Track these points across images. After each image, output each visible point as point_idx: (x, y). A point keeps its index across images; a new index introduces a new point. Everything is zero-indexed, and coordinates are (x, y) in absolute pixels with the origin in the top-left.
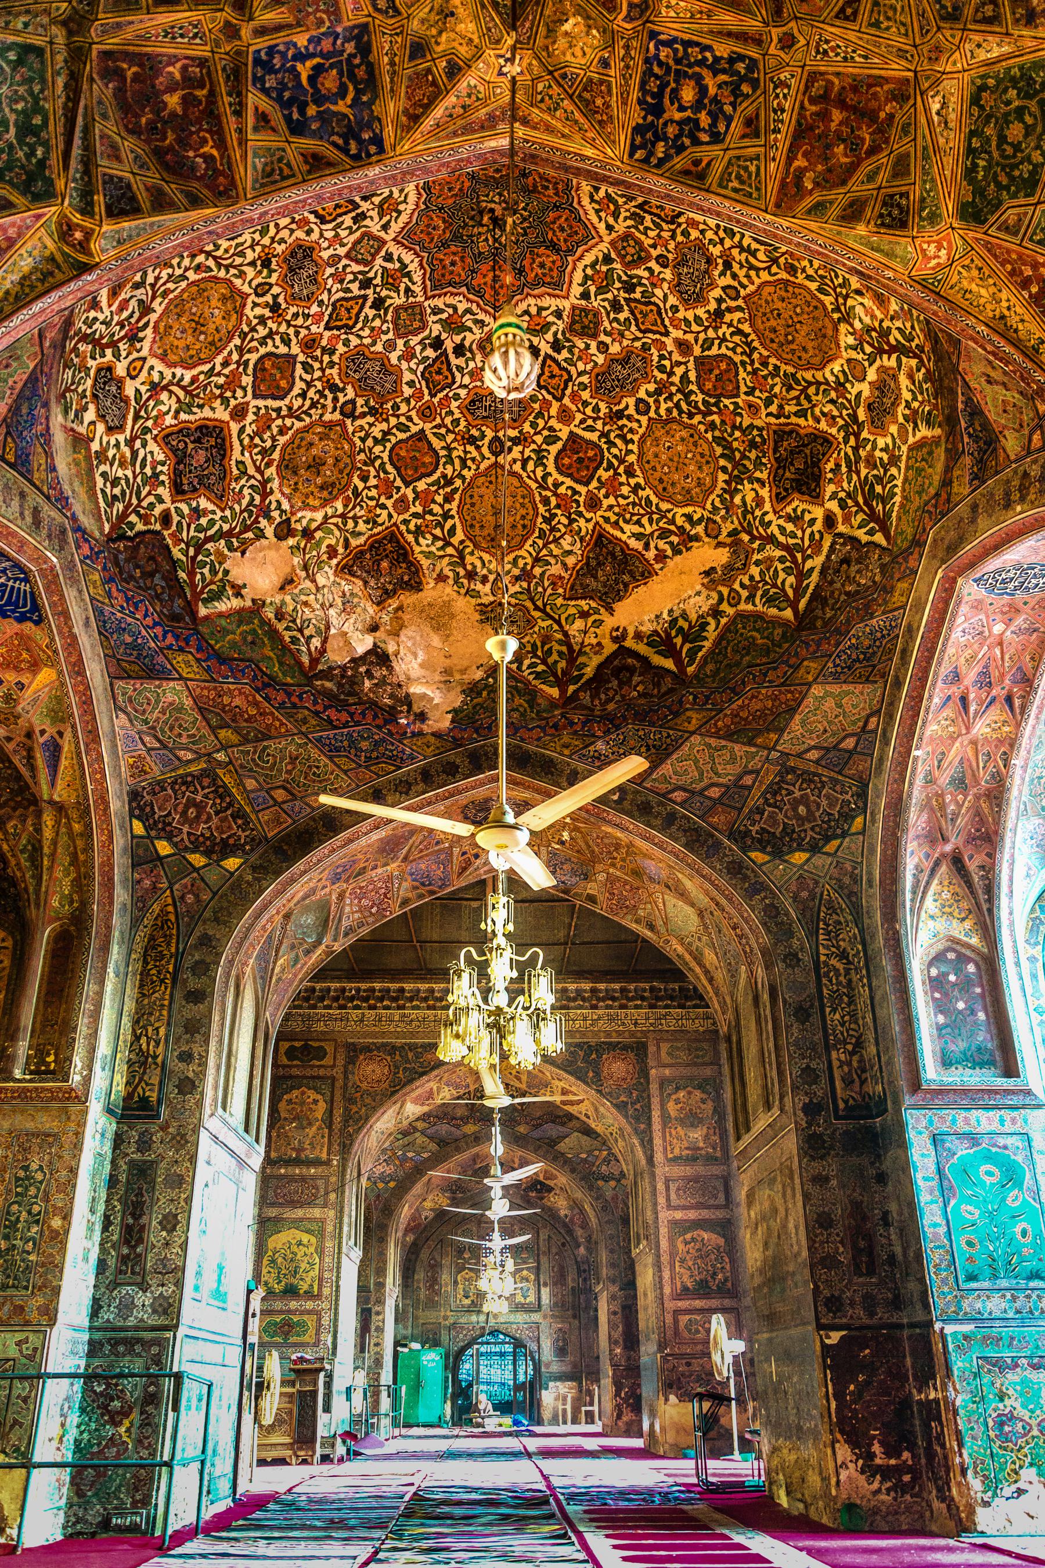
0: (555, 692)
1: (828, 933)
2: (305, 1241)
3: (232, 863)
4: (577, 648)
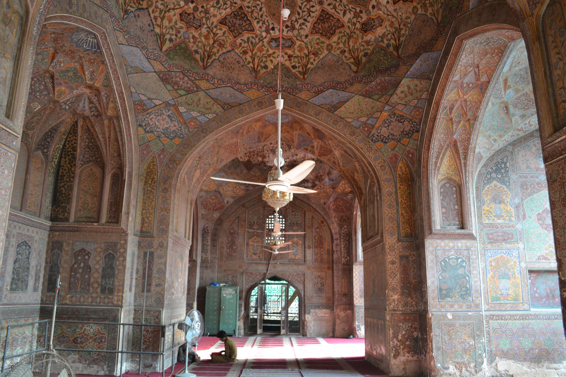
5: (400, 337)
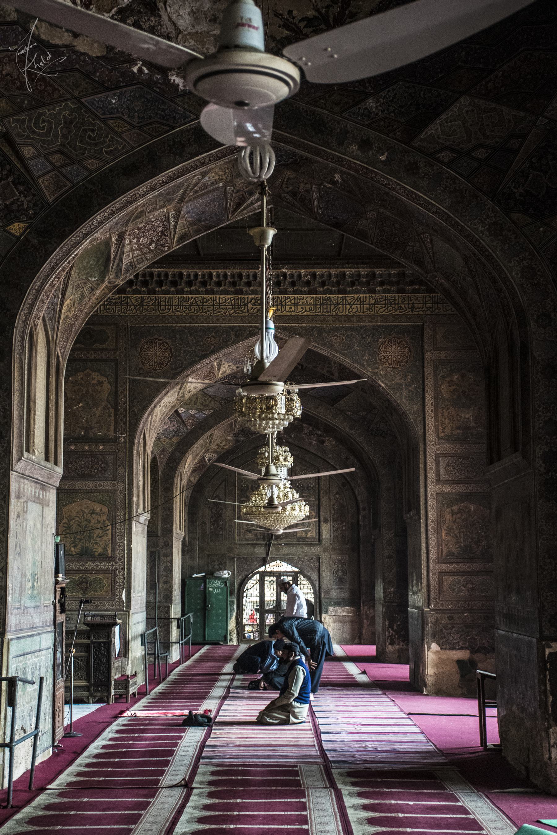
2: (98, 510)
5: (395, 628)
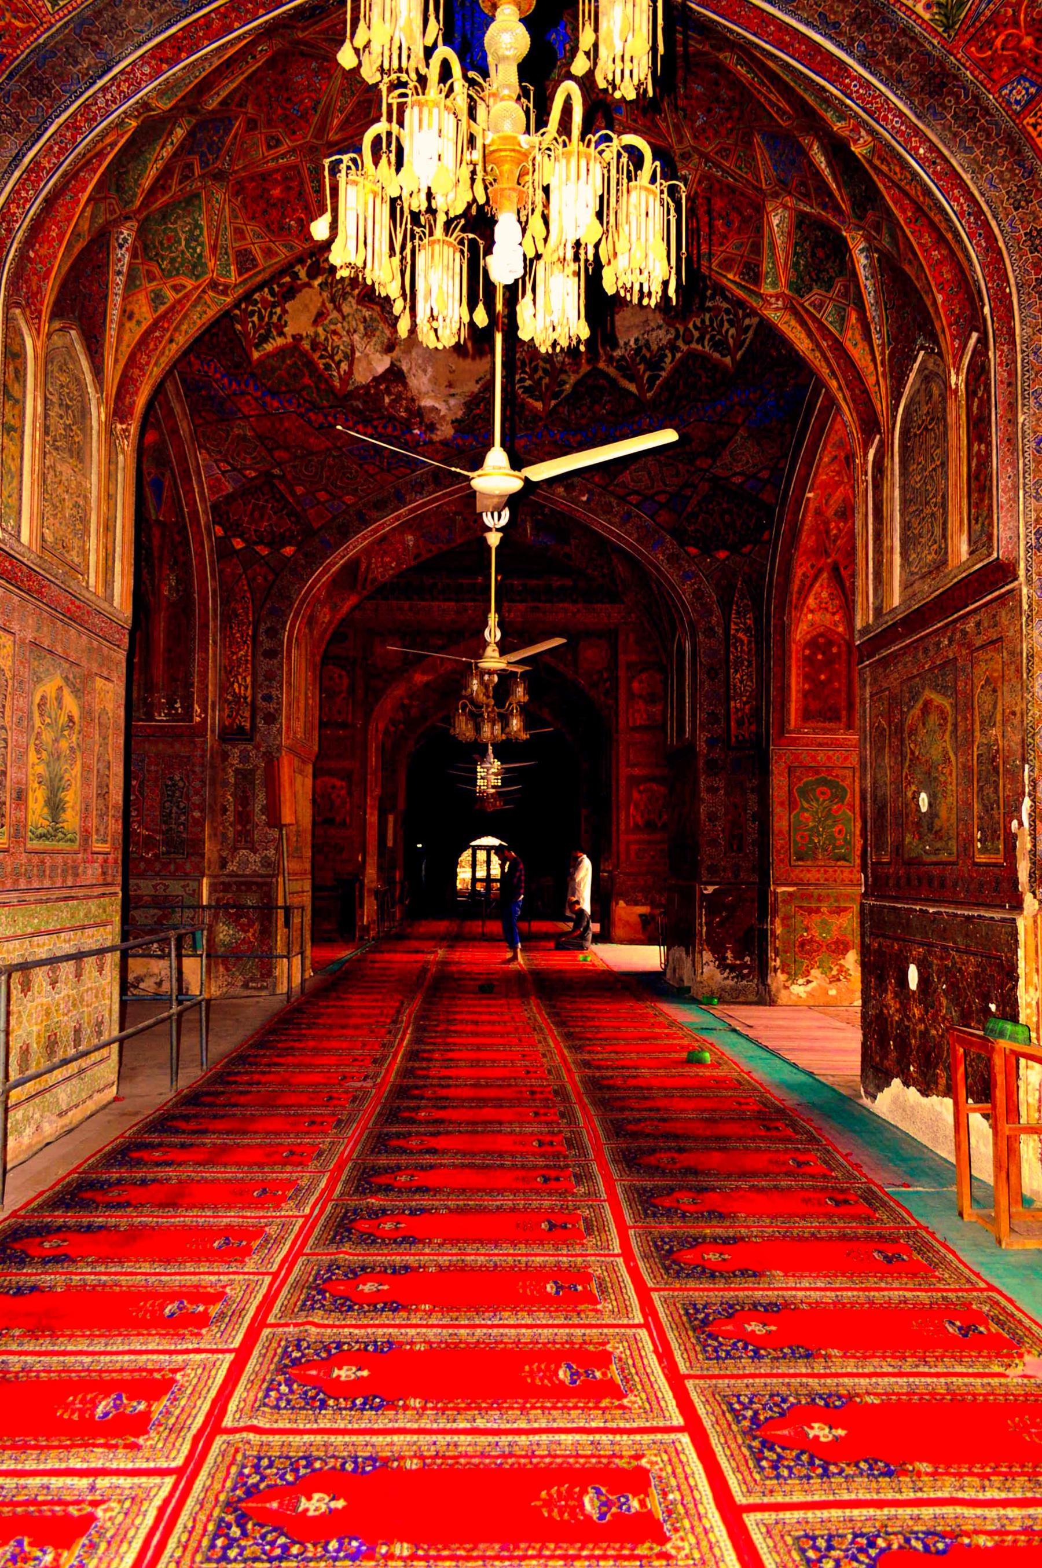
0: (539, 405)
1: (738, 612)
3: (288, 550)
4: (558, 366)
